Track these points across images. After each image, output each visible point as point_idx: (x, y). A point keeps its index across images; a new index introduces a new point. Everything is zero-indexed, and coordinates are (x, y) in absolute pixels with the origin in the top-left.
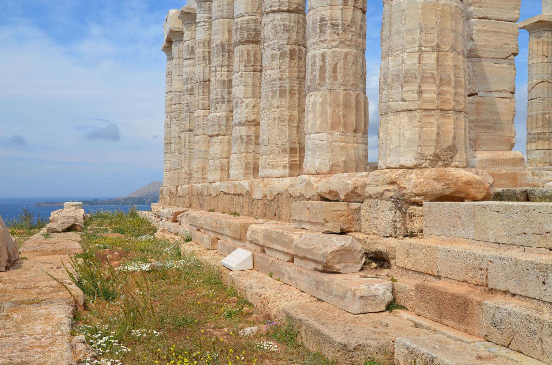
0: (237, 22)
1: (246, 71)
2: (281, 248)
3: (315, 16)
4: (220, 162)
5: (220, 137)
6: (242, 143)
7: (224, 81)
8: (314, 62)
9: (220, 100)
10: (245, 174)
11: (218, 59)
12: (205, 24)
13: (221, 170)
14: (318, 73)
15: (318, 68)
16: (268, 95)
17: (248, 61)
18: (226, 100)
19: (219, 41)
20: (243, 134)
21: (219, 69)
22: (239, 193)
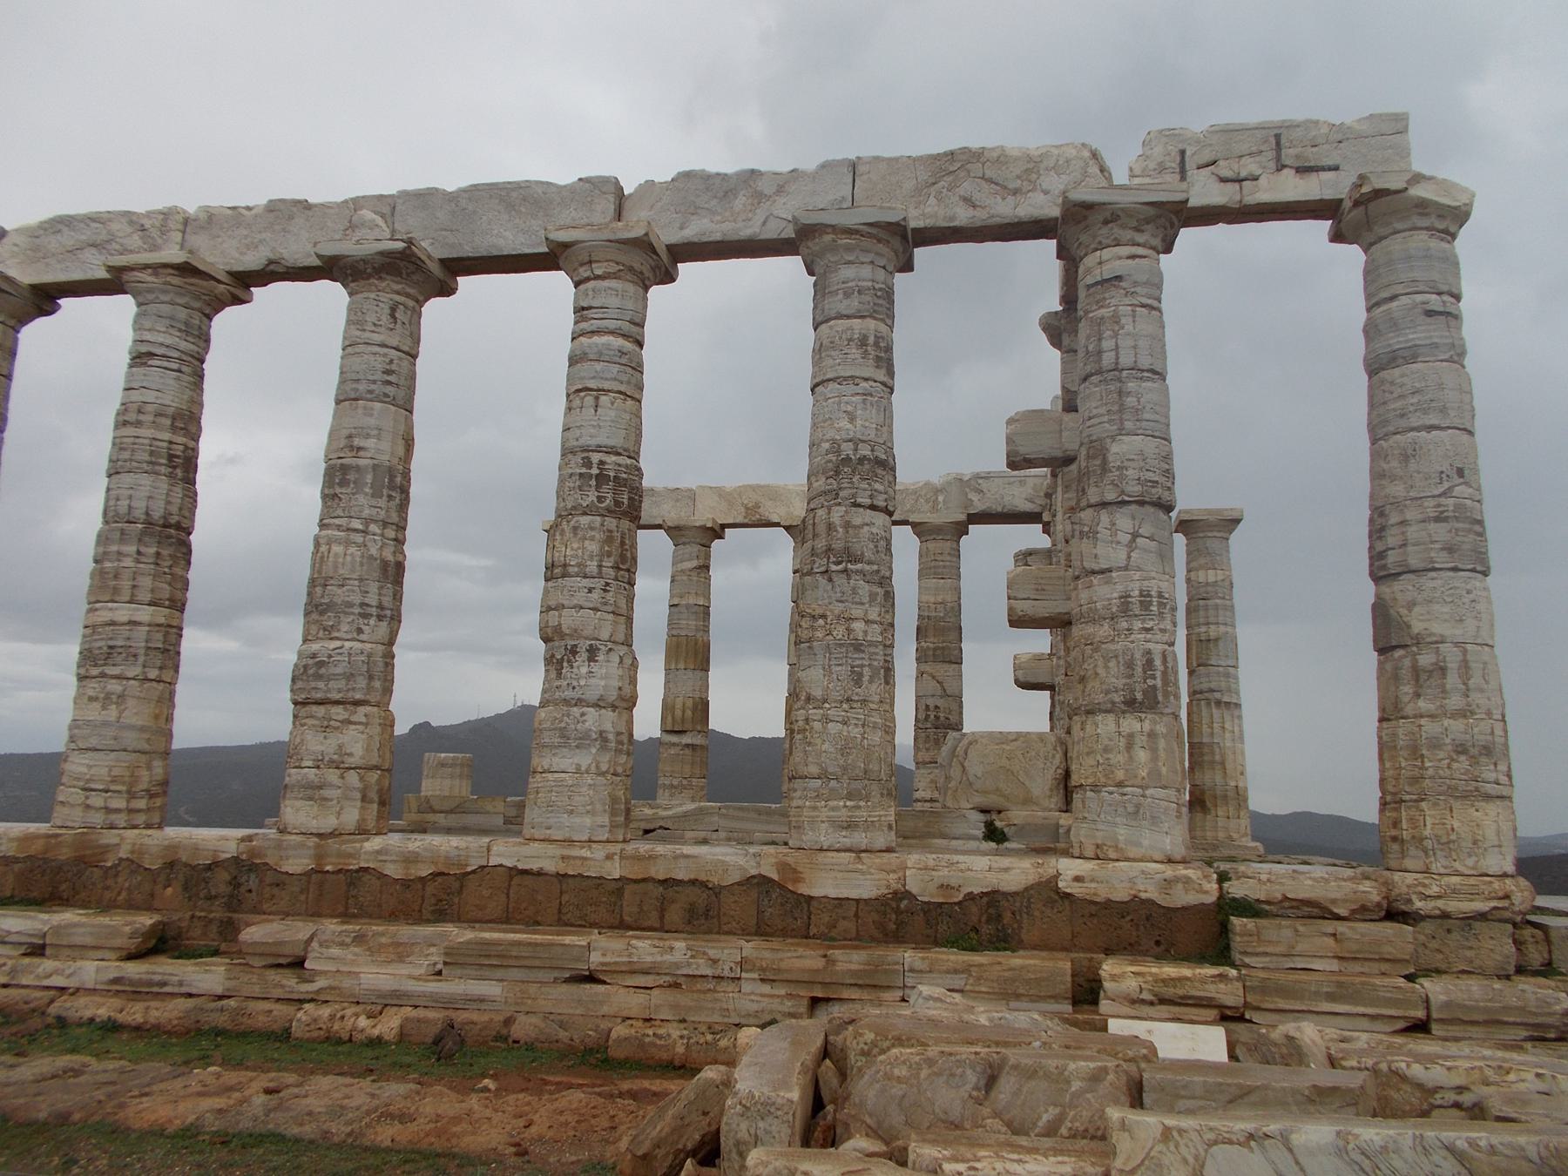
0: (602, 462)
1: (616, 579)
2: (1361, 1010)
3: (1146, 583)
4: (361, 779)
5: (362, 710)
6: (604, 748)
7: (385, 565)
8: (1149, 664)
9: (374, 611)
10: (613, 826)
11: (374, 503)
12: (184, 369)
13: (364, 799)
14: (1159, 683)
15: (1158, 674)
16: (861, 675)
17: (623, 558)
18: (388, 613)
19: (384, 458)
20: (608, 726)
21: (373, 528)
22: (681, 875)
